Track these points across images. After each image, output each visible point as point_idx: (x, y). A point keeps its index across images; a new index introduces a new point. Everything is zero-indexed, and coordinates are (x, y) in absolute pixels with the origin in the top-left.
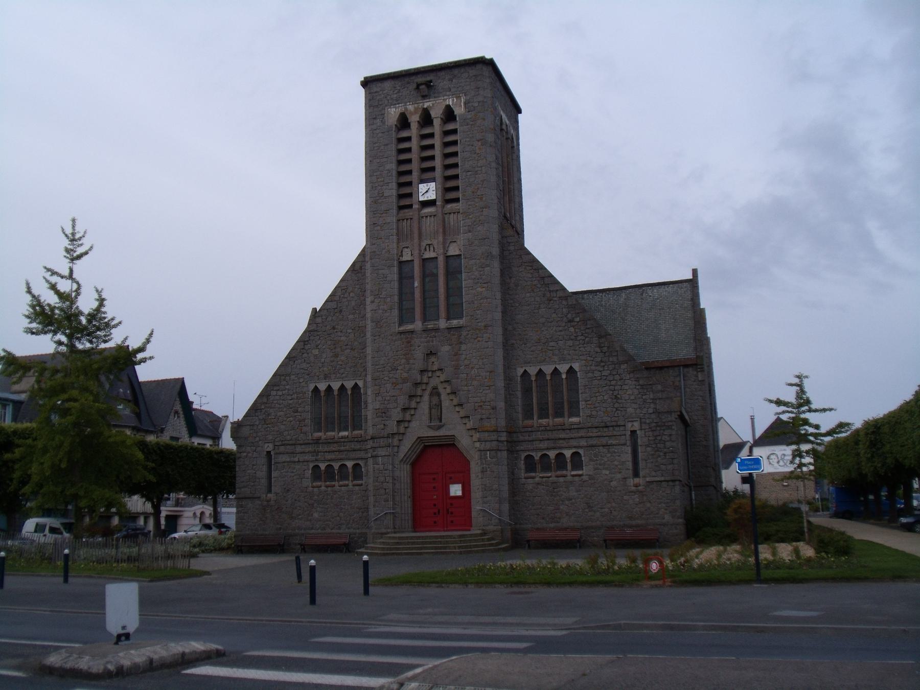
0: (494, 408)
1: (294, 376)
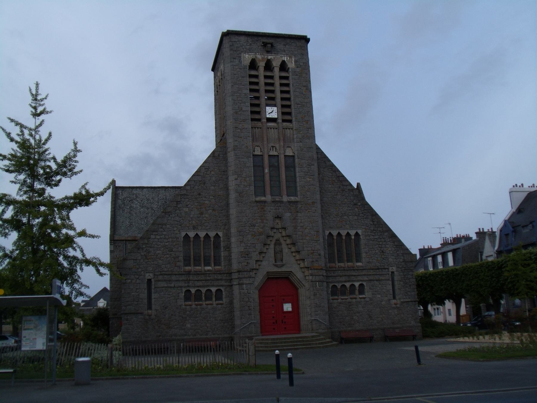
0: (320, 255)
1: (169, 226)
